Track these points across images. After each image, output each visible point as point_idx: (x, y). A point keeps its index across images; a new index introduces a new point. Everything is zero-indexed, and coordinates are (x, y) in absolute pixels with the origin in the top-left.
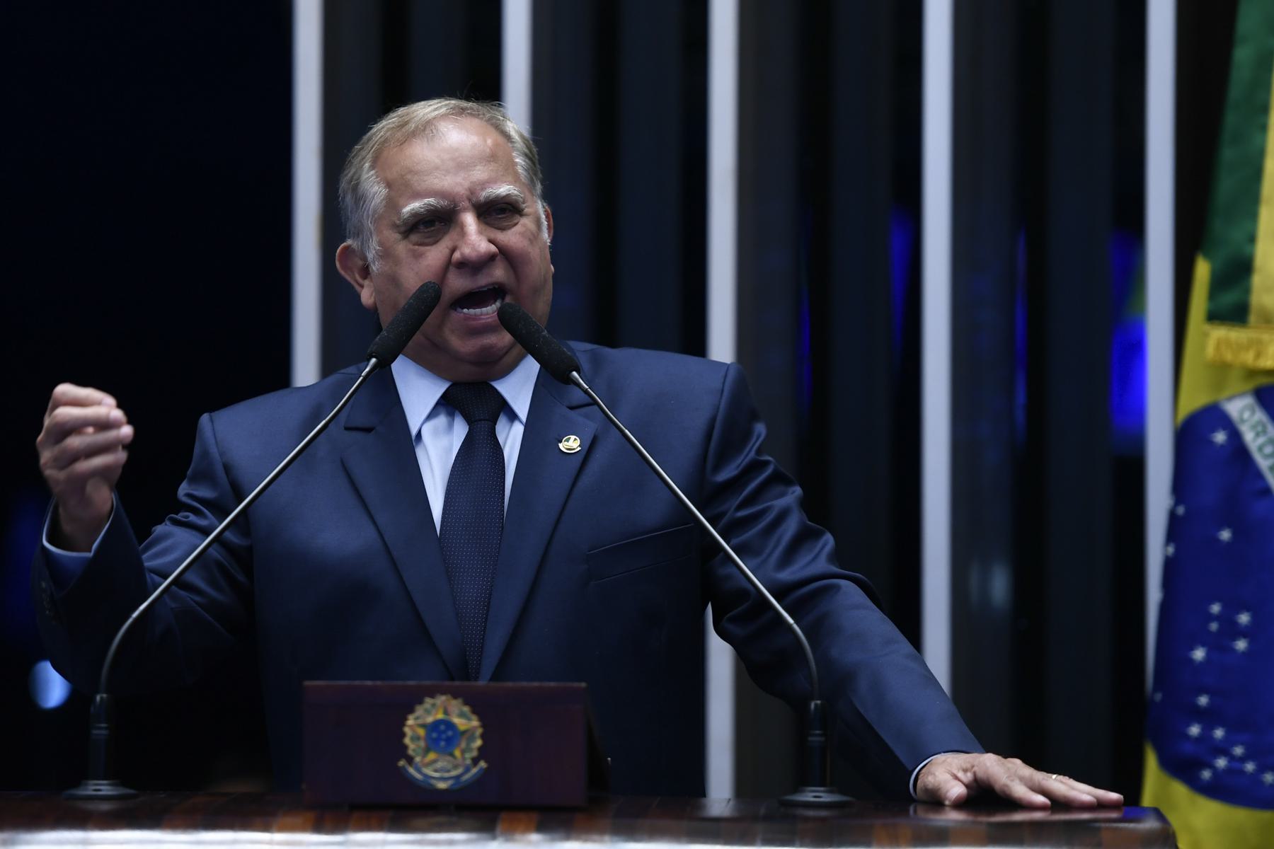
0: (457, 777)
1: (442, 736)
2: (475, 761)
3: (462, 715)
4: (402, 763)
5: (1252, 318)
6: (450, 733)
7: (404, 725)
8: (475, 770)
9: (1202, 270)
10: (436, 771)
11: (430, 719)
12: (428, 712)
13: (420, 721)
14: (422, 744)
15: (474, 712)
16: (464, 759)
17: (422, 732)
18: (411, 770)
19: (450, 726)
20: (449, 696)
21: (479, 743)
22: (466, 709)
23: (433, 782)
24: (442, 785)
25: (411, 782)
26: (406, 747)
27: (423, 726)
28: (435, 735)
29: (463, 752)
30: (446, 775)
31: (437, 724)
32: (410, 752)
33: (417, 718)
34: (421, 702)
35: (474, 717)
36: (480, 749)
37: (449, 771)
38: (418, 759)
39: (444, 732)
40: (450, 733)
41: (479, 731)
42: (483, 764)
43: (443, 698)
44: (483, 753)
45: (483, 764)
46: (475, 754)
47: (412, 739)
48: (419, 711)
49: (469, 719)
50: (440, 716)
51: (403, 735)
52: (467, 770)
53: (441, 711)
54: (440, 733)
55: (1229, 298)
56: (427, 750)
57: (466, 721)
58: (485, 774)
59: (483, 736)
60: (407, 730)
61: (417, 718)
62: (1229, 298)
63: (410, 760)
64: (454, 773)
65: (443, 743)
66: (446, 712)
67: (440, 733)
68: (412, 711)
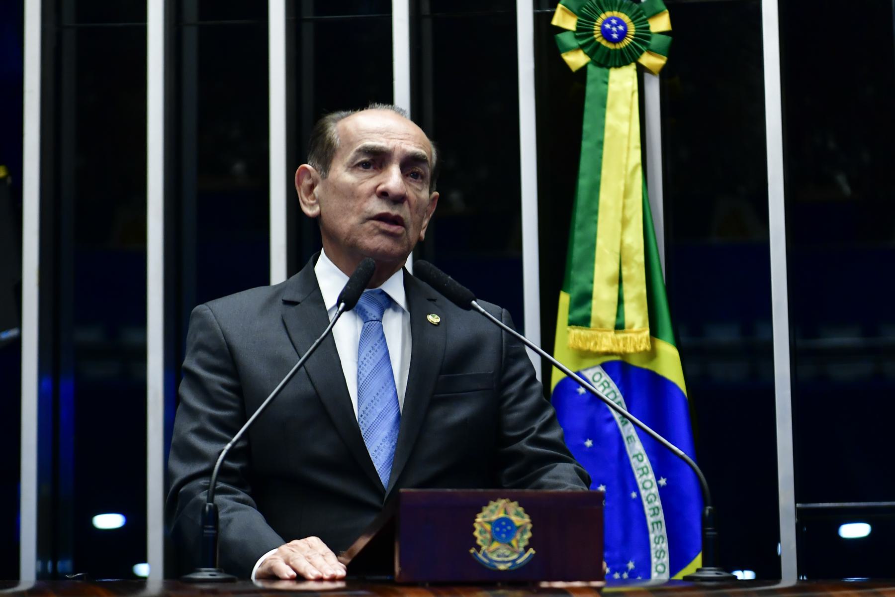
0: (514, 561)
1: (503, 530)
2: (526, 549)
3: (517, 514)
4: (472, 551)
5: (592, 324)
6: (509, 528)
7: (474, 522)
8: (526, 555)
9: (565, 299)
10: (499, 556)
11: (494, 518)
12: (492, 512)
13: (487, 519)
14: (488, 536)
15: (526, 512)
16: (519, 547)
17: (488, 527)
18: (480, 555)
19: (509, 522)
20: (508, 500)
21: (528, 535)
22: (521, 509)
23: (496, 564)
24: (502, 567)
25: (480, 565)
26: (475, 538)
27: (489, 522)
28: (498, 529)
29: (518, 542)
30: (506, 559)
31: (500, 520)
32: (479, 542)
33: (484, 517)
34: (487, 505)
35: (526, 516)
36: (530, 540)
37: (507, 556)
38: (484, 548)
39: (505, 527)
40: (509, 528)
41: (529, 526)
42: (532, 551)
43: (504, 501)
44: (532, 543)
45: (532, 551)
46: (526, 543)
47: (481, 532)
48: (486, 511)
49: (523, 517)
50: (502, 515)
51: (474, 529)
52: (521, 555)
53: (503, 511)
54: (502, 527)
55: (580, 313)
56: (493, 540)
57: (521, 519)
58: (533, 558)
59: (532, 530)
60: (476, 525)
61: (484, 517)
62: (580, 313)
63: (479, 548)
64: (511, 558)
65: (504, 536)
66: (506, 512)
67: (502, 527)
68: (480, 511)
